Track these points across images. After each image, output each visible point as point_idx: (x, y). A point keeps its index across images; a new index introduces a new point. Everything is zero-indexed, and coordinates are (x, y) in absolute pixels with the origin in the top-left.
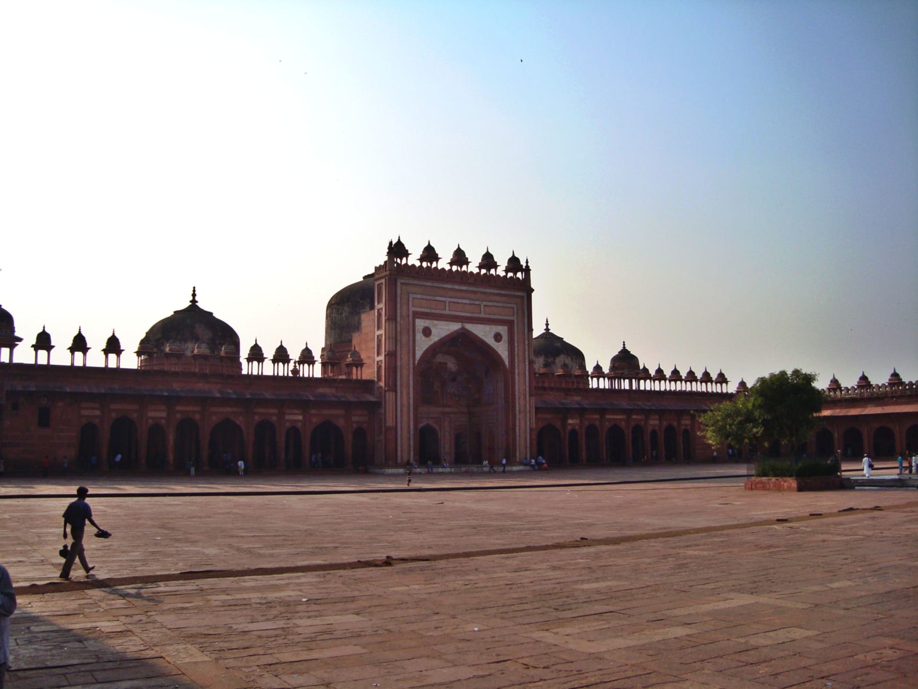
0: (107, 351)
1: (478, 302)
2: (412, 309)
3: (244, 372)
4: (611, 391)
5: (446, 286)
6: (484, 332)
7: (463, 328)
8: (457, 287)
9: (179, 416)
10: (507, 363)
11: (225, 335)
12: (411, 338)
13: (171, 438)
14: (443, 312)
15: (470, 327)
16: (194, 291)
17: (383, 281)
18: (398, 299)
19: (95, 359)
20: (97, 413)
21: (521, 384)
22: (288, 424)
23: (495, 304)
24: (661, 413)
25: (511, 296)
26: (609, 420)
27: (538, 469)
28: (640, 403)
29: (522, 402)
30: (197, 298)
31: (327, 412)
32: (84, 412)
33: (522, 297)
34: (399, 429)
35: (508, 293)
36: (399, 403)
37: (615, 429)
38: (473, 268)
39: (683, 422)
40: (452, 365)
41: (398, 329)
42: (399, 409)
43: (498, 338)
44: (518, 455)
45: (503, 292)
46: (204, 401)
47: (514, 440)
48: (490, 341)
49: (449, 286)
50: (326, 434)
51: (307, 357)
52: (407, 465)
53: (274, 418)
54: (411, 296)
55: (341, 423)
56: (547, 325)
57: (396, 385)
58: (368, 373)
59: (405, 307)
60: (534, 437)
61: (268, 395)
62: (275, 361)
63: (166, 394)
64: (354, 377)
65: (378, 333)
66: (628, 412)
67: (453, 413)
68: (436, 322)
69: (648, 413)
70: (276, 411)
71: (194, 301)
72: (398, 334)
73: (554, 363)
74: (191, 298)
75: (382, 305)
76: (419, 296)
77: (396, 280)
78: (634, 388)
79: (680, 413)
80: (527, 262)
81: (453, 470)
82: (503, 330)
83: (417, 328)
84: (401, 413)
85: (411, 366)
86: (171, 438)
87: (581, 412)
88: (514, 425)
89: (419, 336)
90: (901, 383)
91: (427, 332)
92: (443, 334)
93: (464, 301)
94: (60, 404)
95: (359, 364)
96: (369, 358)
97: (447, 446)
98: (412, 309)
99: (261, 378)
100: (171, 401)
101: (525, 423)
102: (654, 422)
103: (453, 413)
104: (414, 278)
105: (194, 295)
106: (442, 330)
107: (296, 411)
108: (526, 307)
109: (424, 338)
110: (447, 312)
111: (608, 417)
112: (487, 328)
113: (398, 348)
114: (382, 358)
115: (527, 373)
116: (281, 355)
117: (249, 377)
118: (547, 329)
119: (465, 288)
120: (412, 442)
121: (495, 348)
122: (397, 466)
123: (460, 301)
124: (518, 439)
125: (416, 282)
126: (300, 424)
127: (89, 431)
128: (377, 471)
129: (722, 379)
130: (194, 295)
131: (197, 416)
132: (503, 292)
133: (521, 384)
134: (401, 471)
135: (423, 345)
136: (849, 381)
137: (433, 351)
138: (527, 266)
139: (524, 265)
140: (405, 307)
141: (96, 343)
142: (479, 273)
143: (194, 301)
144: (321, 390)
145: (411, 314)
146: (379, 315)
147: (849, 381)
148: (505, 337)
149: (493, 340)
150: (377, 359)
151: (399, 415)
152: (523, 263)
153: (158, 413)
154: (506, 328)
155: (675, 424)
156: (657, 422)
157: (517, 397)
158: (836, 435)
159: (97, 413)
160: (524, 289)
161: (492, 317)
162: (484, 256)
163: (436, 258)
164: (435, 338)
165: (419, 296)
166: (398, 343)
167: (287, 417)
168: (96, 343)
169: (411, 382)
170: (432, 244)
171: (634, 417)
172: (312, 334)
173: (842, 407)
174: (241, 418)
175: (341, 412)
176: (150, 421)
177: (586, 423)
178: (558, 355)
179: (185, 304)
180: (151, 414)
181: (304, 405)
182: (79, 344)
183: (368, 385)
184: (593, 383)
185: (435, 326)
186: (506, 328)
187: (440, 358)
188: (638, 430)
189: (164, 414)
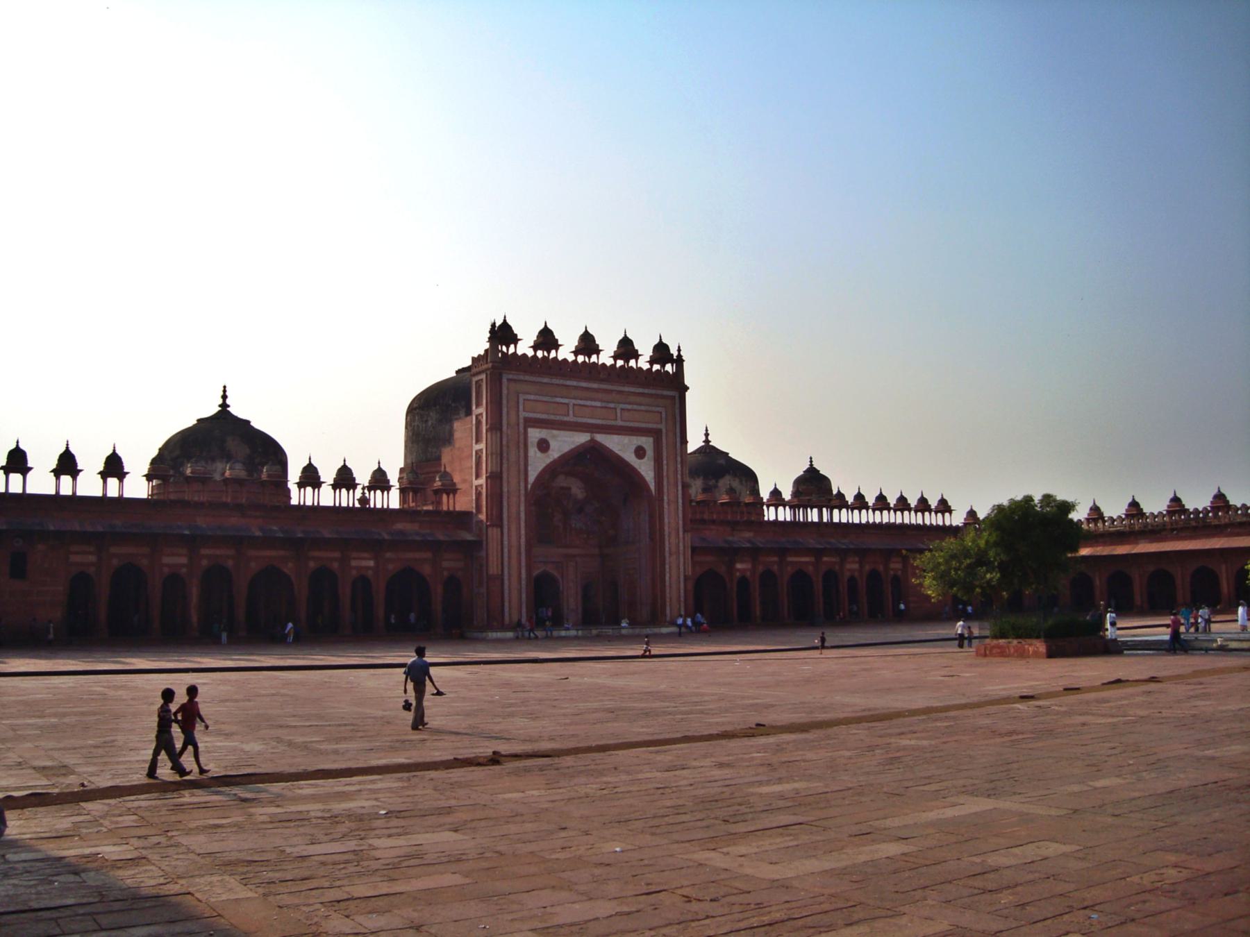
0: (105, 475)
1: (612, 405)
2: (523, 414)
3: (294, 502)
4: (793, 525)
5: (569, 383)
6: (621, 446)
7: (592, 440)
9: (205, 562)
10: (652, 487)
11: (267, 451)
12: (522, 454)
13: (194, 593)
14: (566, 419)
15: (600, 438)
16: (225, 391)
17: (483, 376)
18: (504, 402)
19: (89, 485)
20: (92, 558)
21: (673, 517)
22: (354, 572)
23: (635, 407)
24: (862, 553)
25: (657, 396)
26: (792, 563)
27: (697, 632)
28: (833, 541)
29: (673, 540)
30: (228, 402)
31: (410, 555)
32: (74, 558)
33: (674, 397)
34: (506, 578)
35: (653, 392)
36: (506, 543)
37: (800, 576)
38: (606, 358)
39: (892, 566)
40: (577, 490)
41: (504, 442)
42: (506, 550)
43: (640, 452)
44: (668, 612)
45: (646, 391)
46: (239, 542)
47: (663, 592)
48: (630, 457)
49: (575, 383)
50: (407, 586)
51: (379, 481)
52: (518, 625)
53: (336, 565)
55: (426, 570)
56: (707, 435)
57: (501, 519)
58: (463, 502)
59: (513, 413)
61: (327, 534)
62: (336, 486)
63: (187, 532)
64: (445, 508)
65: (476, 447)
66: (818, 553)
68: (555, 432)
69: (843, 553)
70: (337, 555)
71: (224, 406)
72: (505, 449)
73: (716, 487)
74: (220, 401)
75: (482, 410)
76: (532, 397)
77: (501, 375)
78: (825, 520)
79: (888, 554)
80: (679, 350)
81: (580, 633)
82: (647, 442)
83: (530, 440)
84: (509, 556)
85: (523, 492)
86: (194, 593)
87: (754, 553)
89: (533, 451)
90: (1185, 511)
91: (543, 446)
92: (566, 448)
93: (594, 403)
95: (451, 489)
96: (464, 481)
97: (571, 600)
98: (523, 414)
99: (317, 510)
100: (192, 542)
101: (677, 569)
102: (852, 566)
104: (525, 372)
105: (224, 397)
106: (564, 443)
107: (365, 555)
108: (677, 411)
109: (539, 454)
110: (570, 418)
111: (790, 559)
112: (626, 439)
113: (504, 469)
114: (482, 481)
115: (680, 501)
116: (345, 479)
117: (301, 508)
118: (707, 441)
119: (595, 386)
120: (524, 596)
121: (636, 466)
122: (503, 628)
123: (589, 403)
125: (527, 378)
126: (370, 572)
127: (80, 583)
128: (476, 635)
129: (944, 507)
130: (224, 397)
131: (230, 563)
132: (646, 391)
133: (673, 517)
134: (510, 635)
135: (538, 463)
136: (1114, 509)
137: (551, 471)
138: (679, 356)
139: (675, 354)
141: (91, 464)
142: (613, 366)
143: (224, 406)
144: (399, 526)
145: (521, 421)
146: (479, 423)
147: (1114, 509)
148: (650, 453)
149: (633, 456)
150: (476, 483)
151: (506, 559)
152: (674, 352)
153: (176, 559)
154: (651, 440)
155: (881, 568)
156: (856, 566)
157: (666, 533)
158: (1098, 582)
159: (92, 558)
160: (677, 385)
161: (631, 424)
162: (621, 342)
163: (556, 345)
164: (555, 452)
165: (532, 397)
166: (505, 461)
167: (354, 563)
168: (91, 464)
169: (523, 515)
170: (549, 326)
171: (825, 559)
172: (386, 449)
173: (1105, 544)
174: (290, 565)
175: (428, 555)
176: (166, 570)
177: (761, 569)
178: (722, 476)
179: (212, 409)
180: (166, 560)
181: (375, 547)
182: (67, 465)
183: (463, 518)
184: (770, 514)
185: (554, 437)
187: (562, 481)
188: (831, 577)
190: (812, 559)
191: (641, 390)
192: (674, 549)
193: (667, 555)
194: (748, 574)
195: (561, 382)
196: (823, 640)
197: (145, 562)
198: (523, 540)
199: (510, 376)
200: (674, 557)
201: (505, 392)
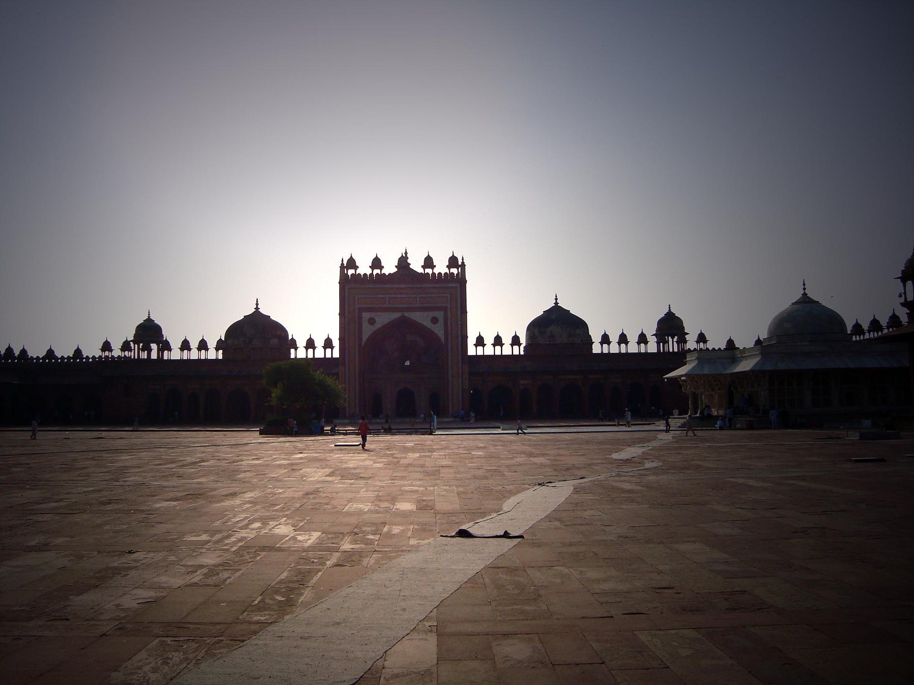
6: (422, 318)
8: (396, 286)
10: (443, 339)
14: (385, 306)
15: (407, 314)
43: (434, 320)
48: (428, 324)
56: (556, 299)
71: (257, 308)
82: (440, 315)
91: (372, 321)
105: (257, 304)
106: (383, 319)
109: (369, 326)
110: (387, 306)
115: (460, 346)
118: (556, 303)
122: (345, 417)
130: (257, 304)
134: (346, 421)
135: (368, 331)
138: (463, 263)
143: (257, 308)
148: (441, 320)
154: (442, 313)
160: (461, 281)
164: (378, 326)
186: (442, 313)
195: (381, 286)
196: (668, 424)
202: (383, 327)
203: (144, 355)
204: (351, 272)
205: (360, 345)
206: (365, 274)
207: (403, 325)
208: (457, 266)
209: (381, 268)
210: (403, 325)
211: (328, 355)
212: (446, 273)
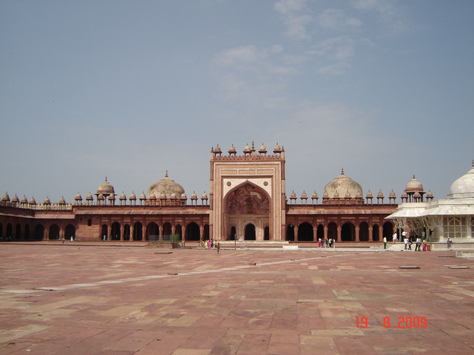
7: (247, 181)
9: (135, 221)
10: (270, 195)
12: (220, 187)
15: (250, 180)
33: (279, 164)
43: (266, 184)
44: (274, 236)
53: (171, 221)
54: (220, 169)
55: (198, 223)
60: (284, 227)
67: (263, 218)
70: (171, 219)
76: (224, 169)
82: (269, 180)
88: (273, 222)
89: (225, 186)
91: (229, 184)
94: (94, 218)
101: (278, 221)
103: (263, 218)
106: (236, 183)
107: (180, 218)
110: (238, 175)
112: (260, 180)
124: (274, 229)
132: (267, 163)
135: (227, 190)
140: (217, 175)
145: (220, 177)
148: (270, 184)
153: (127, 221)
157: (274, 210)
169: (220, 206)
175: (199, 218)
177: (329, 221)
180: (125, 221)
186: (271, 179)
189: (129, 221)
190: (355, 218)
191: (265, 163)
192: (277, 215)
193: (274, 217)
194: (323, 223)
197: (119, 222)
198: (220, 213)
199: (216, 163)
200: (278, 218)
201: (214, 168)
202: (236, 187)
203: (102, 203)
204: (218, 155)
205: (222, 198)
206: (225, 156)
207: (248, 185)
208: (280, 152)
209: (235, 153)
210: (248, 185)
211: (205, 204)
212: (273, 156)
